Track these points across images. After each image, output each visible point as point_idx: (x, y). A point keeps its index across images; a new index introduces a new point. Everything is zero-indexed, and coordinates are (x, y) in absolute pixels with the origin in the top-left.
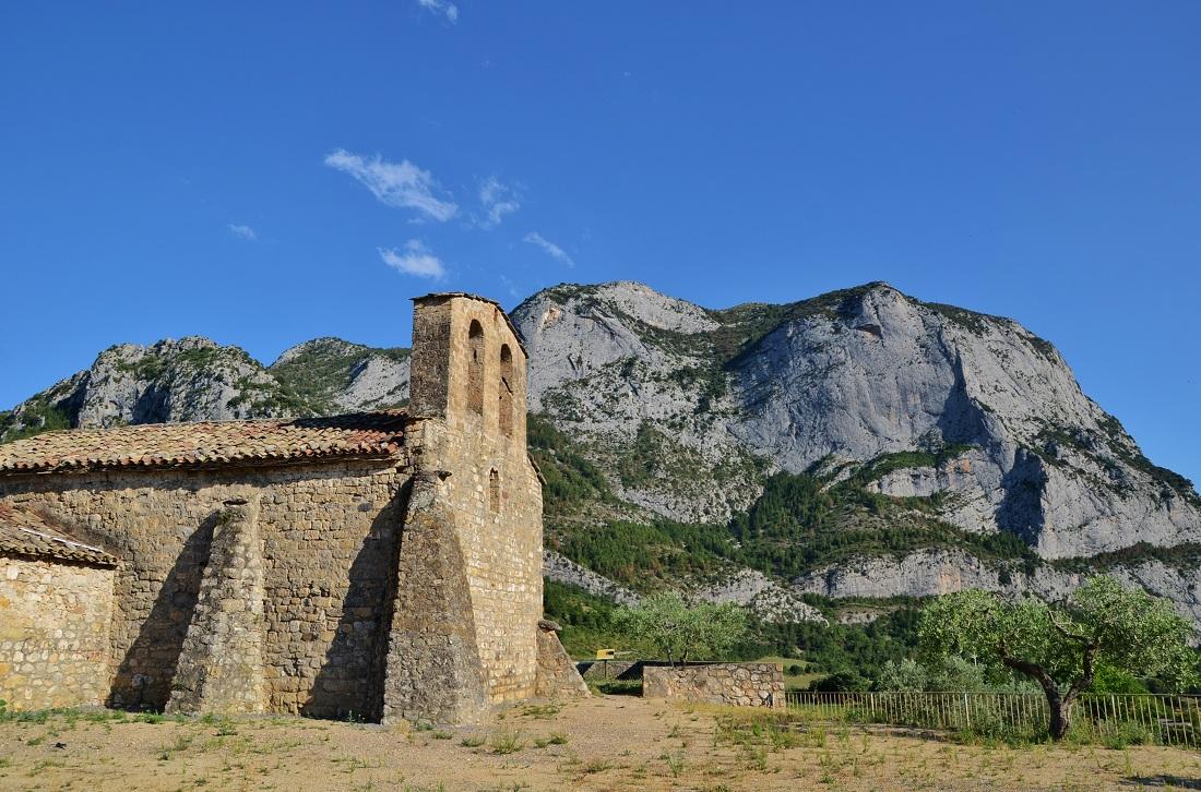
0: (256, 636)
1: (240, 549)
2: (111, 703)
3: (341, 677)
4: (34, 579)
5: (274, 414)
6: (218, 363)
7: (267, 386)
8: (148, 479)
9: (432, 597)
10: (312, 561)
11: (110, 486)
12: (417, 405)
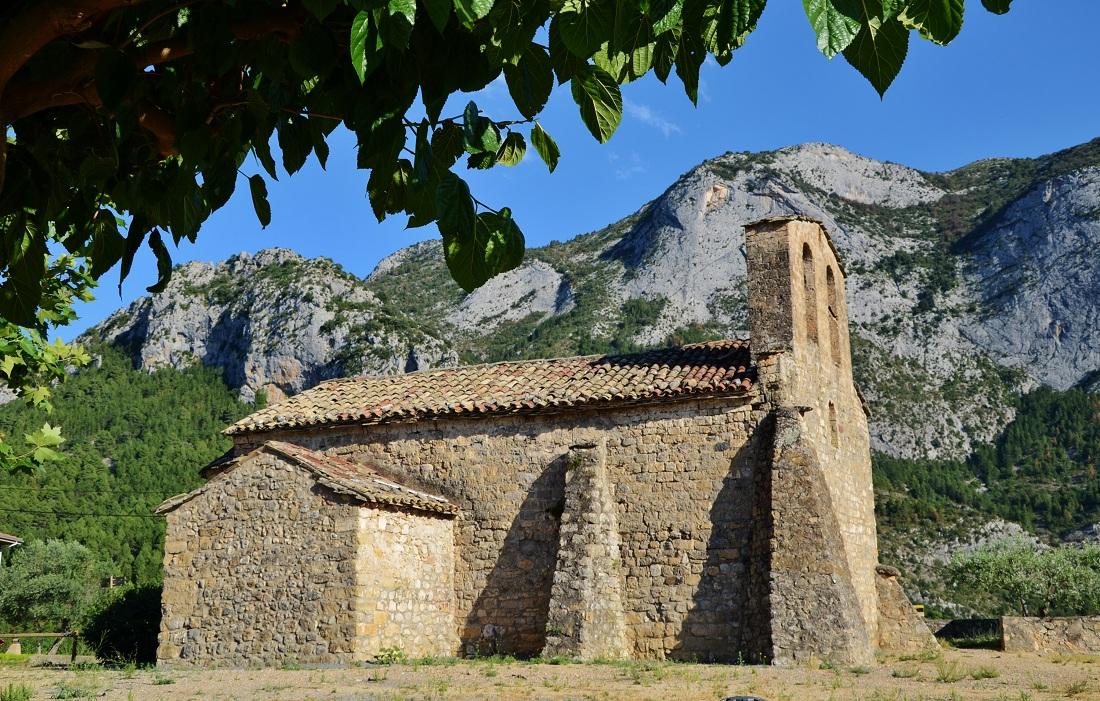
0: (615, 582)
1: (595, 494)
2: (464, 652)
3: (710, 620)
5: (377, 340)
6: (306, 279)
7: (366, 305)
8: (481, 426)
9: (809, 536)
10: (669, 504)
11: (439, 435)
12: (759, 338)
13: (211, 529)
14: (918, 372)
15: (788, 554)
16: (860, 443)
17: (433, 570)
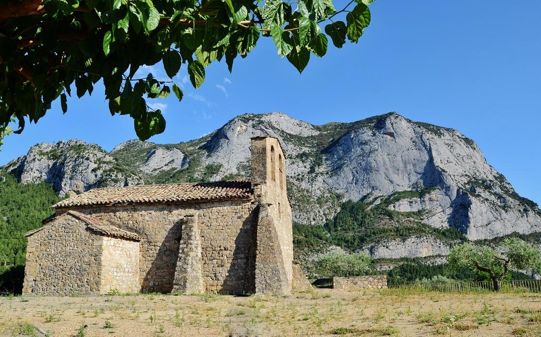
0: (200, 266)
1: (193, 233)
2: (142, 291)
4: (118, 245)
5: (113, 175)
6: (87, 151)
7: (110, 162)
11: (135, 210)
13: (45, 243)
14: (309, 194)
15: (262, 256)
16: (289, 217)
17: (131, 261)
